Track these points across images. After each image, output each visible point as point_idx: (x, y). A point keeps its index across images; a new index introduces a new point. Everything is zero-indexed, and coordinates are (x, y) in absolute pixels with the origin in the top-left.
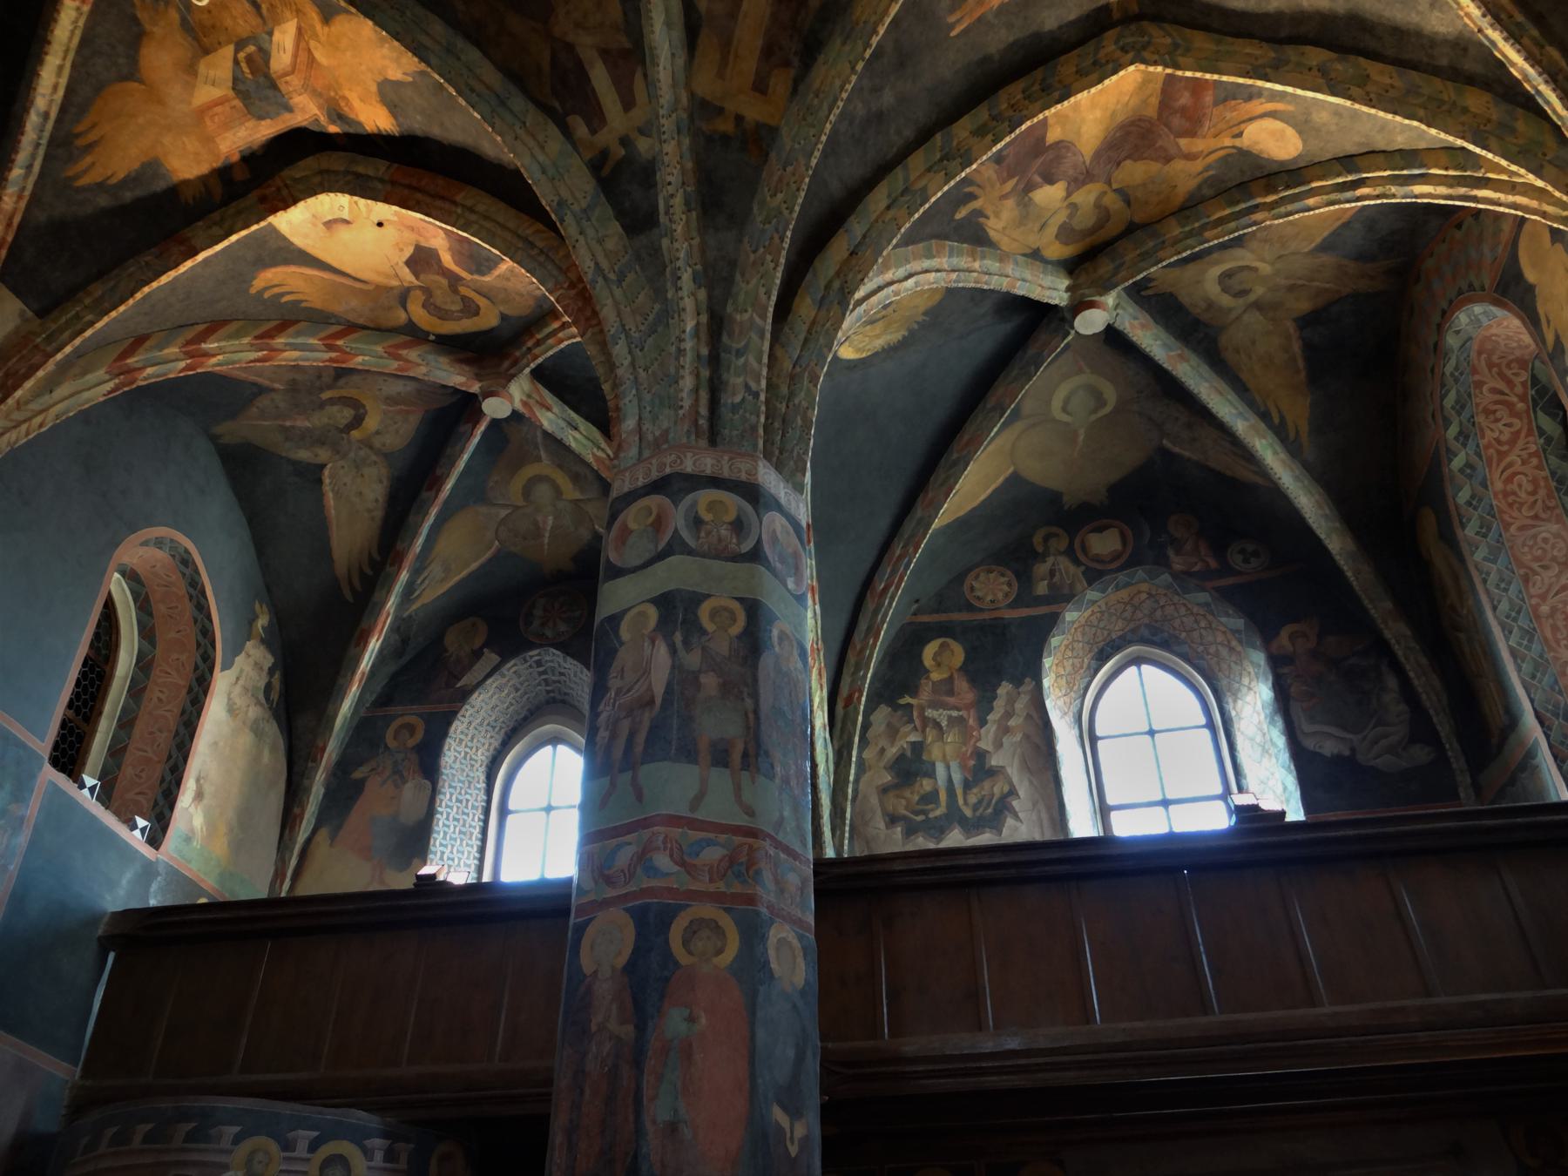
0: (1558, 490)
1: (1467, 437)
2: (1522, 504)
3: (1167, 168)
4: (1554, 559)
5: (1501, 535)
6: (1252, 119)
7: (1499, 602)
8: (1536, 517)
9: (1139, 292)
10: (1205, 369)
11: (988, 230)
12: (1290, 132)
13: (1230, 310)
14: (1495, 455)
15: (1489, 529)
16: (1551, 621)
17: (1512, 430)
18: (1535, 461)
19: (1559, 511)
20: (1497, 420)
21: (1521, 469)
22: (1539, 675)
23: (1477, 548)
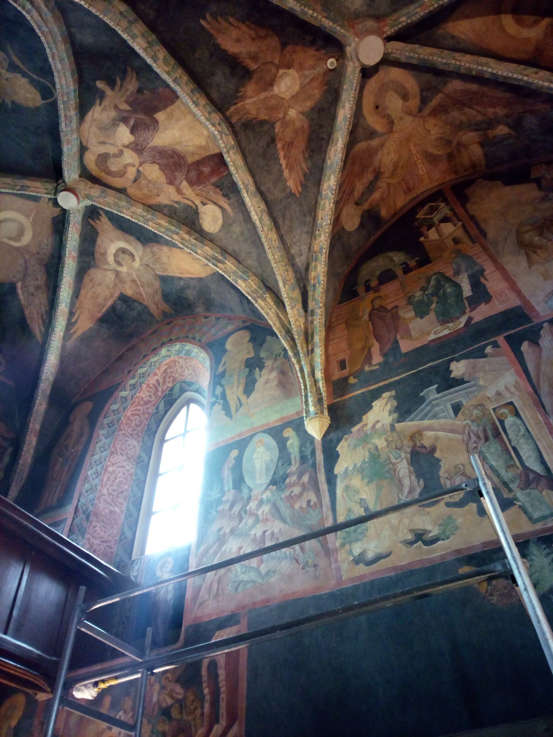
0: (146, 431)
1: (134, 388)
2: (130, 426)
3: (166, 186)
4: (127, 454)
5: (115, 431)
6: (215, 204)
7: (96, 454)
8: (132, 435)
9: (89, 217)
10: (73, 273)
11: (92, 110)
12: (220, 222)
13: (108, 264)
14: (137, 403)
15: (113, 426)
16: (109, 475)
17: (150, 399)
18: (147, 416)
19: (141, 439)
20: (149, 392)
21: (141, 415)
22: (89, 492)
23: (103, 429)
